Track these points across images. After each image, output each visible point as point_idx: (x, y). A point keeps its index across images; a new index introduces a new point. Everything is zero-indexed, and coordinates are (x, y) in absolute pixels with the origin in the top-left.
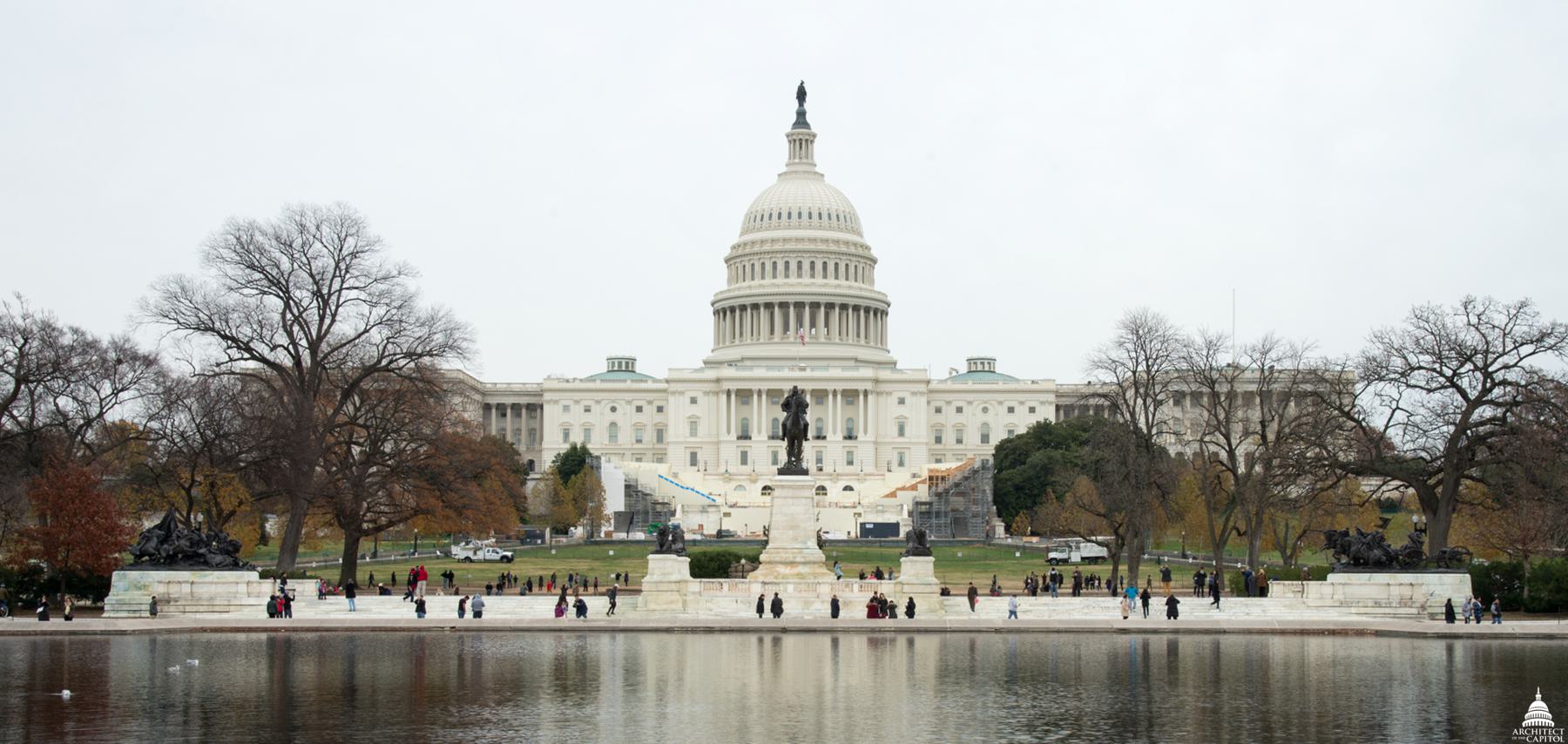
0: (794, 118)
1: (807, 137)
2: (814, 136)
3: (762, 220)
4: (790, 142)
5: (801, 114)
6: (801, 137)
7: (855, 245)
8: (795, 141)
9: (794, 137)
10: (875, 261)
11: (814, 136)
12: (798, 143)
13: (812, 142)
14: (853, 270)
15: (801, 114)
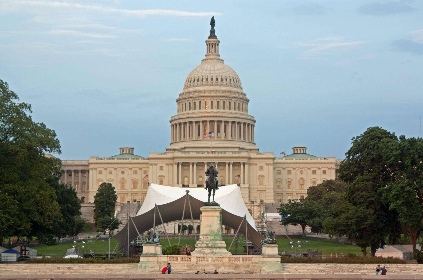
0: (209, 34)
1: (215, 42)
2: (219, 42)
3: (194, 82)
4: (207, 45)
5: (213, 32)
6: (212, 42)
7: (238, 93)
8: (210, 44)
9: (209, 43)
10: (248, 101)
11: (219, 42)
12: (211, 46)
13: (218, 45)
14: (238, 105)
15: (213, 32)
